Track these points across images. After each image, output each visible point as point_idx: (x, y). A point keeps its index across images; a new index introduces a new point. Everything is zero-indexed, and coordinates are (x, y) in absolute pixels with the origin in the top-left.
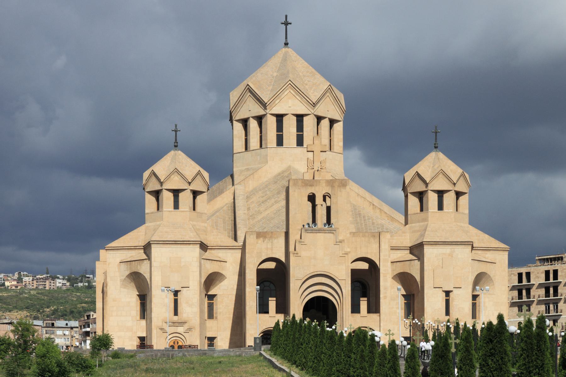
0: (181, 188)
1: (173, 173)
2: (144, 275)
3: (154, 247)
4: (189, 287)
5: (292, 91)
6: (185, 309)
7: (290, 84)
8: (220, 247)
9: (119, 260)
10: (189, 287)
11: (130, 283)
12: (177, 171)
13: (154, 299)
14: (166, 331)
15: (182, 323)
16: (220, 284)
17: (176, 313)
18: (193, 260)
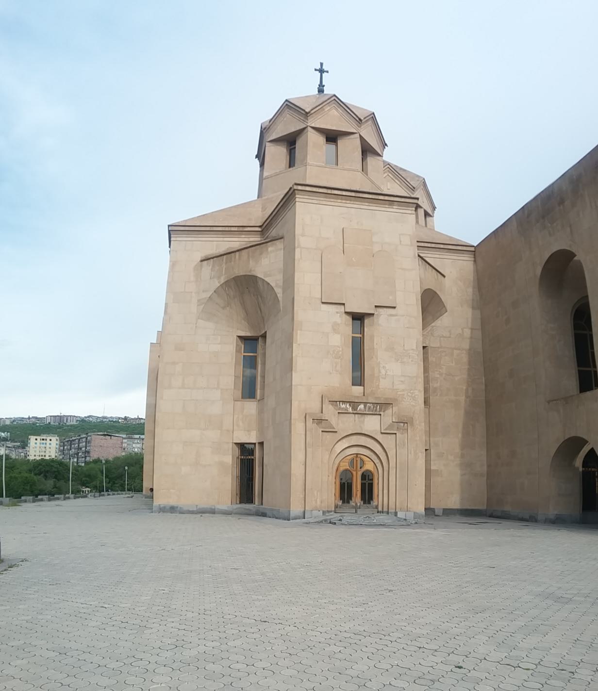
0: (344, 130)
1: (328, 101)
2: (266, 279)
3: (301, 200)
4: (394, 308)
5: (390, 175)
6: (383, 367)
7: (388, 167)
8: (429, 245)
9: (199, 256)
10: (394, 308)
11: (224, 308)
12: (337, 99)
13: (299, 332)
14: (334, 428)
15: (381, 406)
16: (433, 324)
17: (358, 380)
18: (401, 241)
